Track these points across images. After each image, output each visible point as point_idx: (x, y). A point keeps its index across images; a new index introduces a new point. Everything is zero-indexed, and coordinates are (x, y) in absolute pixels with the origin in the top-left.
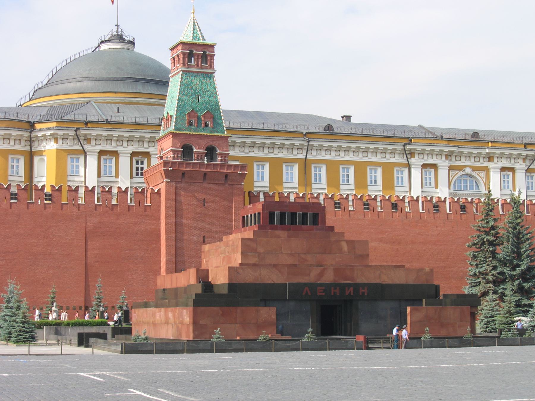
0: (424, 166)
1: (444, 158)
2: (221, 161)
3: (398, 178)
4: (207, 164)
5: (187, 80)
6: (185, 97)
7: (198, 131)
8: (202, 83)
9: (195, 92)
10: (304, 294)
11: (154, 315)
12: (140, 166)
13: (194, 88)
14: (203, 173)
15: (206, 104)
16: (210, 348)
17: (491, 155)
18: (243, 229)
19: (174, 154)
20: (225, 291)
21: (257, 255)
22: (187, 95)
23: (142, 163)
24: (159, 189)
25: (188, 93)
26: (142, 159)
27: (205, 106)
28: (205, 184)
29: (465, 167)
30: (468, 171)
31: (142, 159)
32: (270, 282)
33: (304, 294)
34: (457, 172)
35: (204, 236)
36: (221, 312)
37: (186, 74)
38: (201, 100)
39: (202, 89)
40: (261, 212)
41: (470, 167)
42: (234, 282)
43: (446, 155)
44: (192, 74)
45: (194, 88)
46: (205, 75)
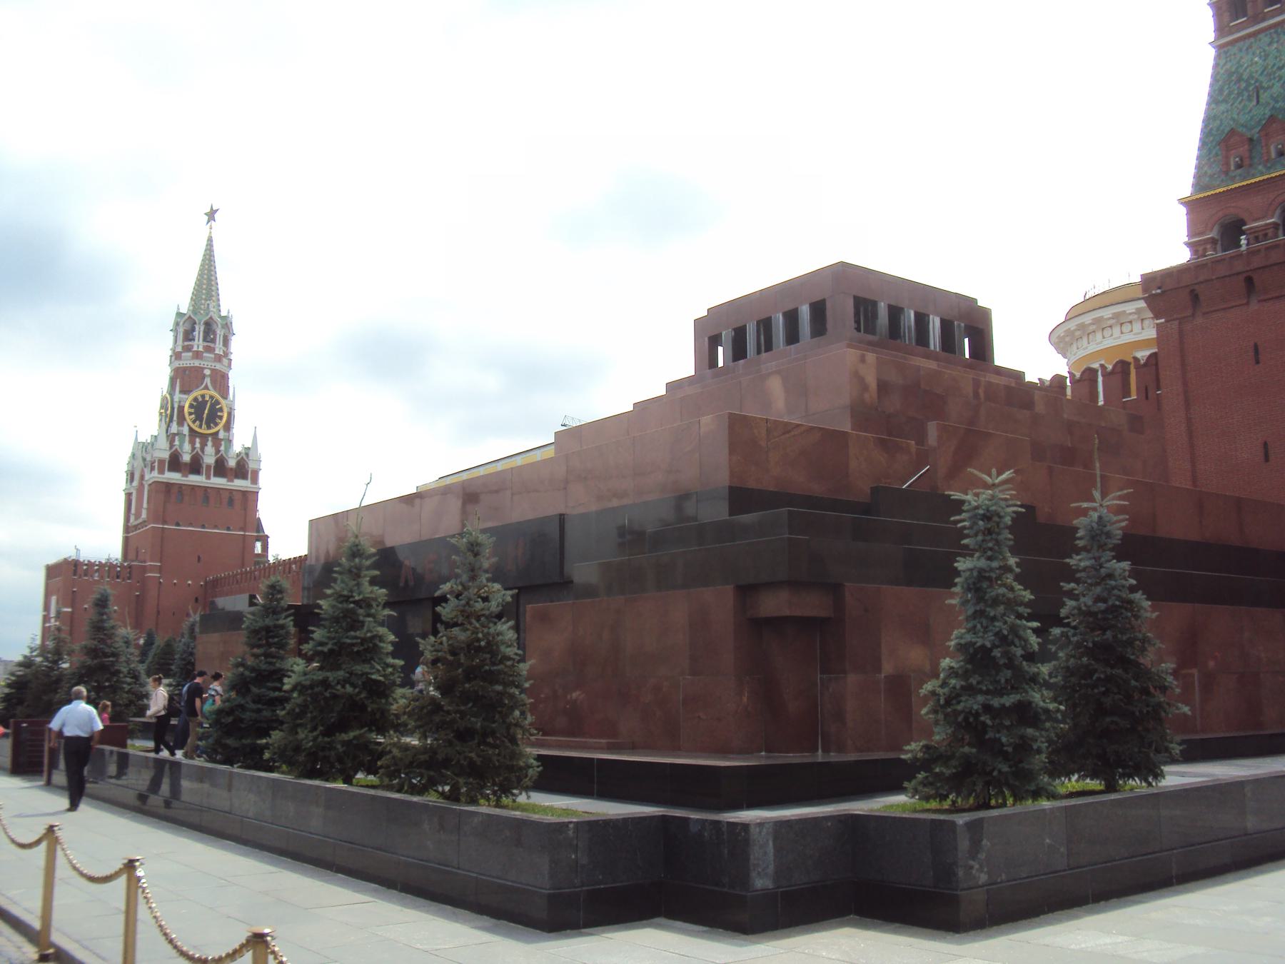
4: (1251, 253)
5: (1228, 66)
6: (1223, 107)
7: (1254, 176)
8: (1267, 56)
9: (1248, 85)
13: (1245, 77)
14: (1242, 277)
15: (1277, 102)
22: (1225, 101)
25: (1230, 93)
27: (1274, 108)
28: (1254, 306)
35: (1265, 444)
37: (1226, 53)
38: (1265, 97)
39: (1265, 69)
44: (1240, 44)
45: (1245, 77)
46: (1276, 32)
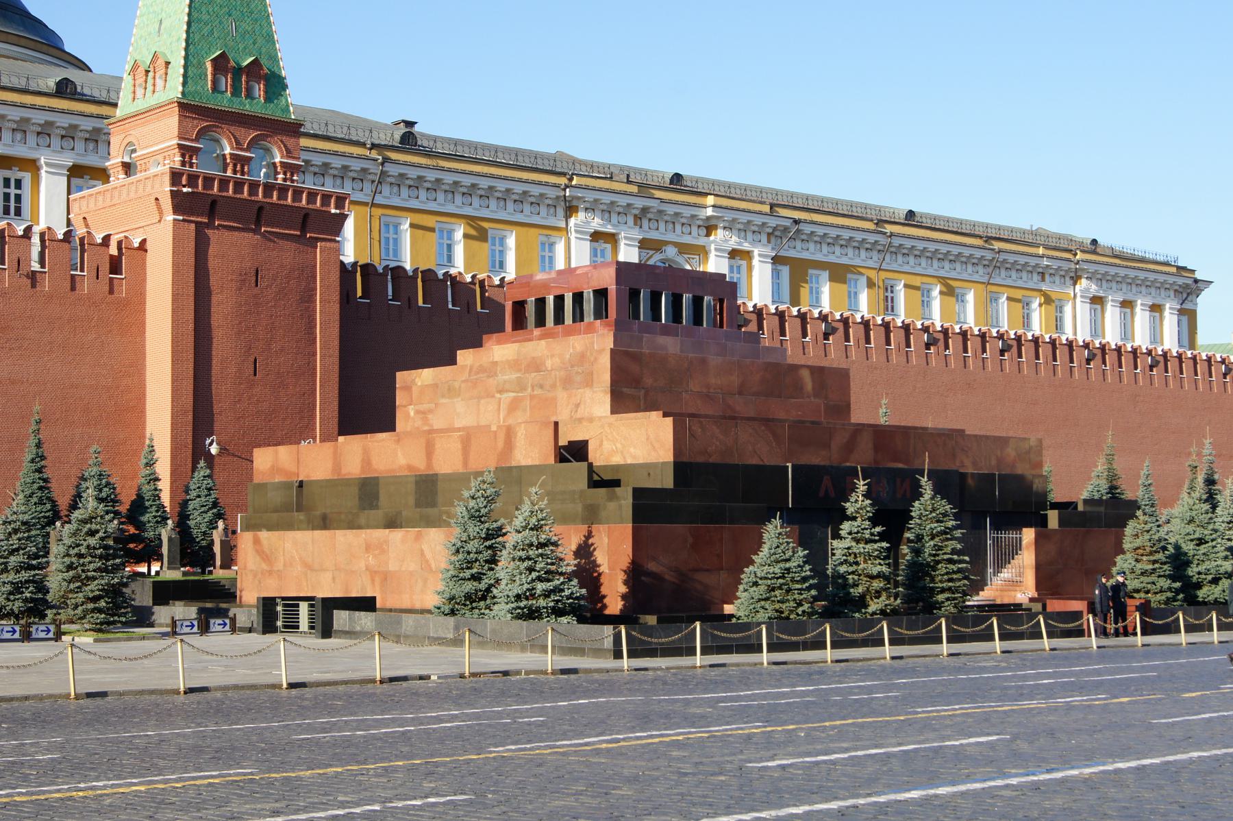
0: (596, 236)
1: (631, 220)
2: (285, 180)
3: (543, 257)
10: (821, 494)
11: (382, 548)
12: (13, 191)
14: (256, 207)
16: (451, 636)
17: (713, 222)
18: (537, 332)
19: (183, 156)
20: (669, 483)
21: (643, 392)
23: (19, 184)
24: (144, 241)
26: (20, 175)
29: (667, 243)
30: (671, 252)
31: (20, 175)
32: (754, 461)
33: (821, 494)
34: (651, 252)
36: (690, 540)
40: (612, 288)
41: (676, 244)
42: (685, 460)
43: (635, 216)
